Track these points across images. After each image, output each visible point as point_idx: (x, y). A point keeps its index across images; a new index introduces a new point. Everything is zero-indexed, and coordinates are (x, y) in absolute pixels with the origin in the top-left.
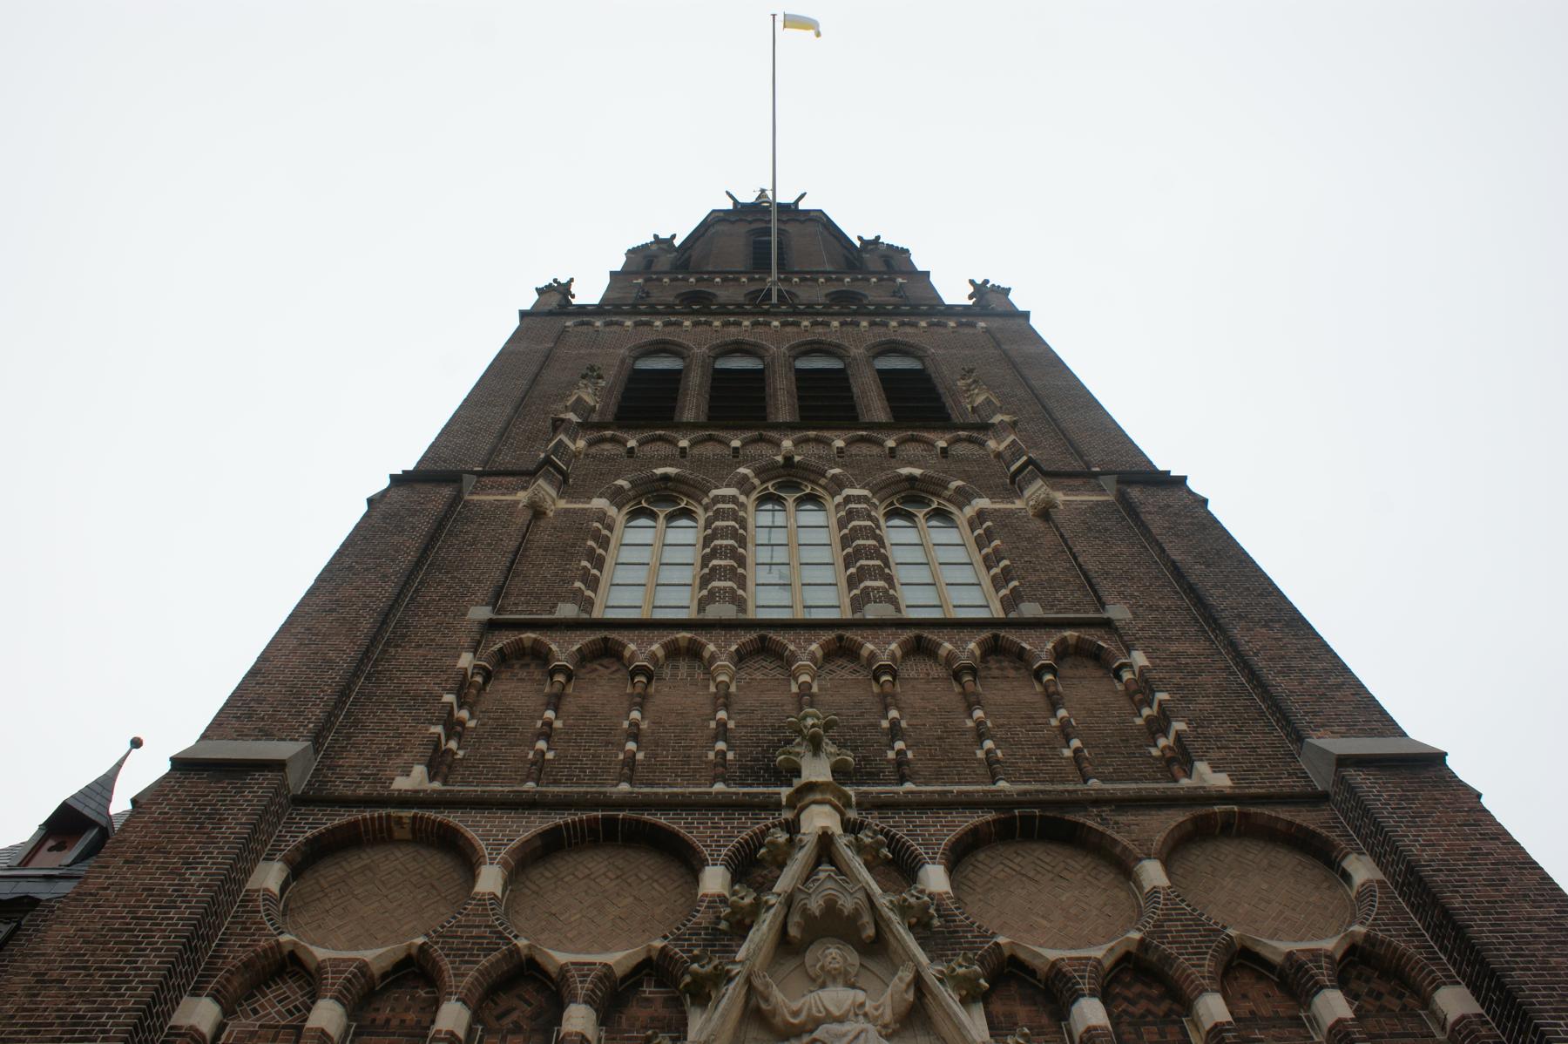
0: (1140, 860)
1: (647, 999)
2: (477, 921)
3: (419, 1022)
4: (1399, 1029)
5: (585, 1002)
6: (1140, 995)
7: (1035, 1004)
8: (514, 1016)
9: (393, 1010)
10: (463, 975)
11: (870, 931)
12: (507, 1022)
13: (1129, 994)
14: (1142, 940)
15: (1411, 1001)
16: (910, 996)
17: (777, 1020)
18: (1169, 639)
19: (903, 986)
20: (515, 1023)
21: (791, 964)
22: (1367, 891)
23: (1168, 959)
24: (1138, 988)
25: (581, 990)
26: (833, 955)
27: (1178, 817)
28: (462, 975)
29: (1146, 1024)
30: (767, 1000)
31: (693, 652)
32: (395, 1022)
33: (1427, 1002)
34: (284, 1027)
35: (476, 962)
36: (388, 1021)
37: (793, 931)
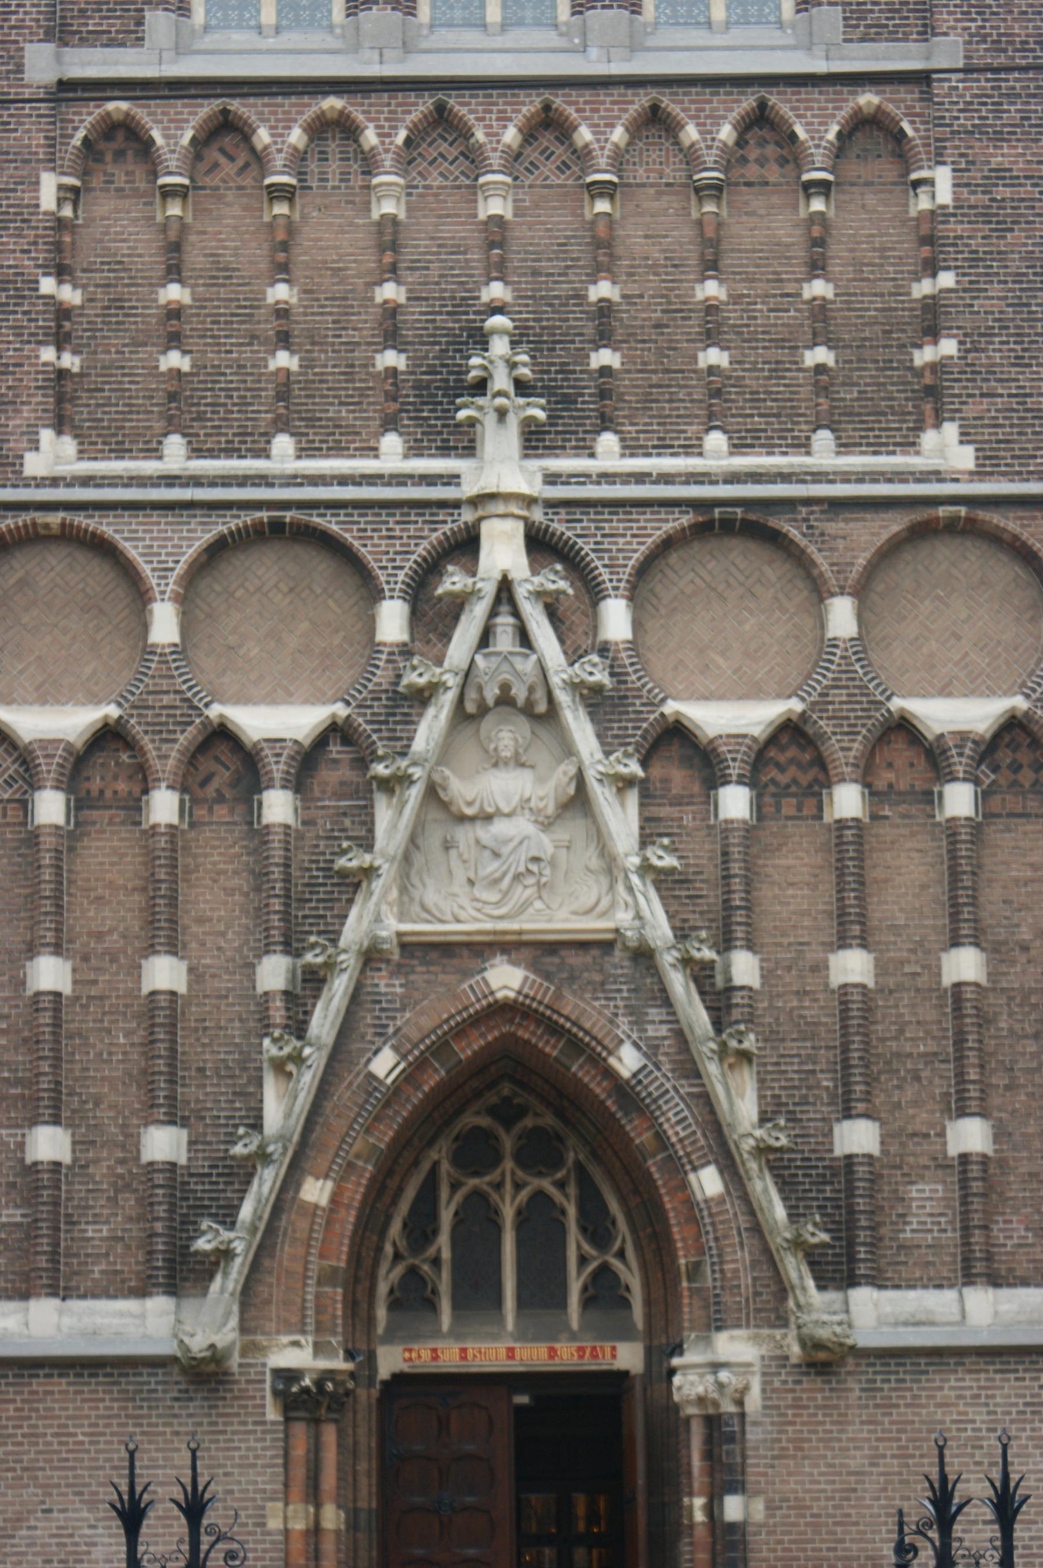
0: (833, 595)
1: (335, 761)
2: (165, 685)
3: (130, 793)
4: (1019, 809)
5: (284, 787)
6: (792, 761)
7: (691, 767)
8: (215, 784)
9: (102, 778)
10: (166, 757)
11: (542, 707)
12: (210, 791)
13: (782, 758)
14: (804, 712)
16: (571, 790)
17: (454, 809)
18: (999, 137)
19: (566, 779)
20: (217, 791)
21: (469, 730)
23: (822, 736)
24: (792, 752)
25: (278, 769)
26: (507, 734)
27: (895, 524)
28: (166, 756)
29: (788, 795)
30: (445, 789)
31: (346, 129)
32: (108, 794)
34: (9, 801)
35: (175, 741)
36: (102, 792)
37: (470, 707)
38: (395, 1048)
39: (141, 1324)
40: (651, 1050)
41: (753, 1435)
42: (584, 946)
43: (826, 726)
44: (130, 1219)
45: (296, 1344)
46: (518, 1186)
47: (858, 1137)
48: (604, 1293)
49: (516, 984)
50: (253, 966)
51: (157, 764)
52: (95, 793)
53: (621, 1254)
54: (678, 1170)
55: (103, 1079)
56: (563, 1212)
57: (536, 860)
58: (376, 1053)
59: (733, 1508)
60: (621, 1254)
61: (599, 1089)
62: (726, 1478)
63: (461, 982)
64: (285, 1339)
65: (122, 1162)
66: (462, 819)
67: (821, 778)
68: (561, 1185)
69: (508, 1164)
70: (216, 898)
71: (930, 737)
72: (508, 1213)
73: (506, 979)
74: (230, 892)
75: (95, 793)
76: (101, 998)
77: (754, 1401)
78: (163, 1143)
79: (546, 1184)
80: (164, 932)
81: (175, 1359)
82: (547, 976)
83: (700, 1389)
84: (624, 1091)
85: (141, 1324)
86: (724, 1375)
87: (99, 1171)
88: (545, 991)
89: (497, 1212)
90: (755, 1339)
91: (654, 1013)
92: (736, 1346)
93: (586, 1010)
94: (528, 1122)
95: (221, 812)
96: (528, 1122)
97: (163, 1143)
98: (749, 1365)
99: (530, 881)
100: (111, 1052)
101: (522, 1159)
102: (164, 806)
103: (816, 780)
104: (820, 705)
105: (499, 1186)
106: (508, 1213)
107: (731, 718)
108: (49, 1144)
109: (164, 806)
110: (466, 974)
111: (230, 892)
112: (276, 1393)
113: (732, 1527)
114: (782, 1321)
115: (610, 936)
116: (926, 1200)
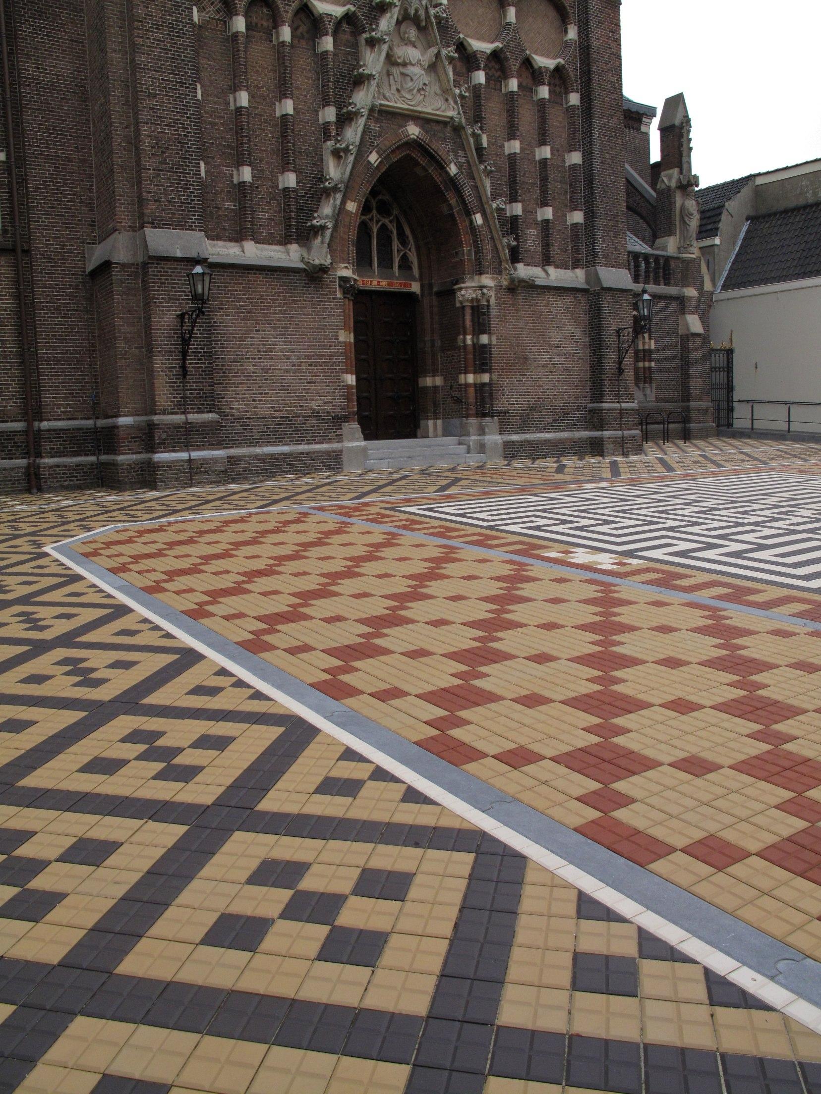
0: (510, 5)
1: (345, 31)
8: (300, 30)
15: (562, 90)
17: (393, 59)
22: (567, 44)
23: (507, 59)
33: (567, 93)
35: (290, 5)
38: (377, 152)
39: (289, 256)
40: (460, 166)
41: (493, 313)
42: (438, 122)
43: (509, 55)
44: (276, 212)
45: (346, 267)
46: (377, 222)
47: (517, 209)
48: (405, 265)
49: (417, 134)
50: (317, 111)
51: (284, 15)
52: (254, 24)
53: (410, 250)
54: (468, 213)
55: (263, 150)
56: (392, 232)
57: (425, 84)
58: (371, 153)
59: (484, 339)
60: (410, 250)
61: (438, 180)
62: (481, 327)
63: (399, 129)
64: (343, 265)
65: (272, 187)
66: (398, 64)
67: (505, 75)
68: (391, 222)
69: (374, 212)
70: (303, 78)
71: (536, 67)
72: (375, 230)
73: (413, 130)
74: (308, 78)
75: (254, 24)
76: (260, 115)
77: (493, 301)
78: (290, 180)
79: (386, 221)
80: (283, 90)
81: (305, 270)
82: (427, 132)
83: (474, 296)
84: (452, 182)
85: (289, 256)
86: (485, 291)
87: (263, 190)
88: (427, 139)
89: (371, 230)
90: (492, 278)
91: (461, 153)
92: (487, 280)
93: (442, 149)
94: (380, 197)
95: (303, 43)
96: (380, 197)
97: (290, 180)
98: (491, 287)
99: (423, 93)
100: (265, 139)
101: (379, 211)
102: (286, 33)
103: (500, 76)
104: (507, 46)
105: (371, 219)
106: (375, 230)
107: (482, 46)
108: (246, 174)
109: (286, 33)
110: (401, 126)
111: (308, 78)
112: (340, 286)
113: (484, 346)
114: (500, 273)
115: (448, 120)
116: (532, 235)
